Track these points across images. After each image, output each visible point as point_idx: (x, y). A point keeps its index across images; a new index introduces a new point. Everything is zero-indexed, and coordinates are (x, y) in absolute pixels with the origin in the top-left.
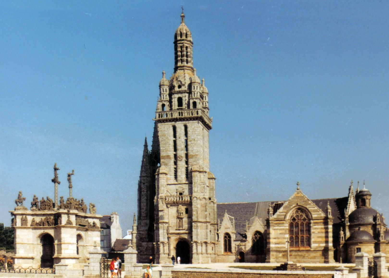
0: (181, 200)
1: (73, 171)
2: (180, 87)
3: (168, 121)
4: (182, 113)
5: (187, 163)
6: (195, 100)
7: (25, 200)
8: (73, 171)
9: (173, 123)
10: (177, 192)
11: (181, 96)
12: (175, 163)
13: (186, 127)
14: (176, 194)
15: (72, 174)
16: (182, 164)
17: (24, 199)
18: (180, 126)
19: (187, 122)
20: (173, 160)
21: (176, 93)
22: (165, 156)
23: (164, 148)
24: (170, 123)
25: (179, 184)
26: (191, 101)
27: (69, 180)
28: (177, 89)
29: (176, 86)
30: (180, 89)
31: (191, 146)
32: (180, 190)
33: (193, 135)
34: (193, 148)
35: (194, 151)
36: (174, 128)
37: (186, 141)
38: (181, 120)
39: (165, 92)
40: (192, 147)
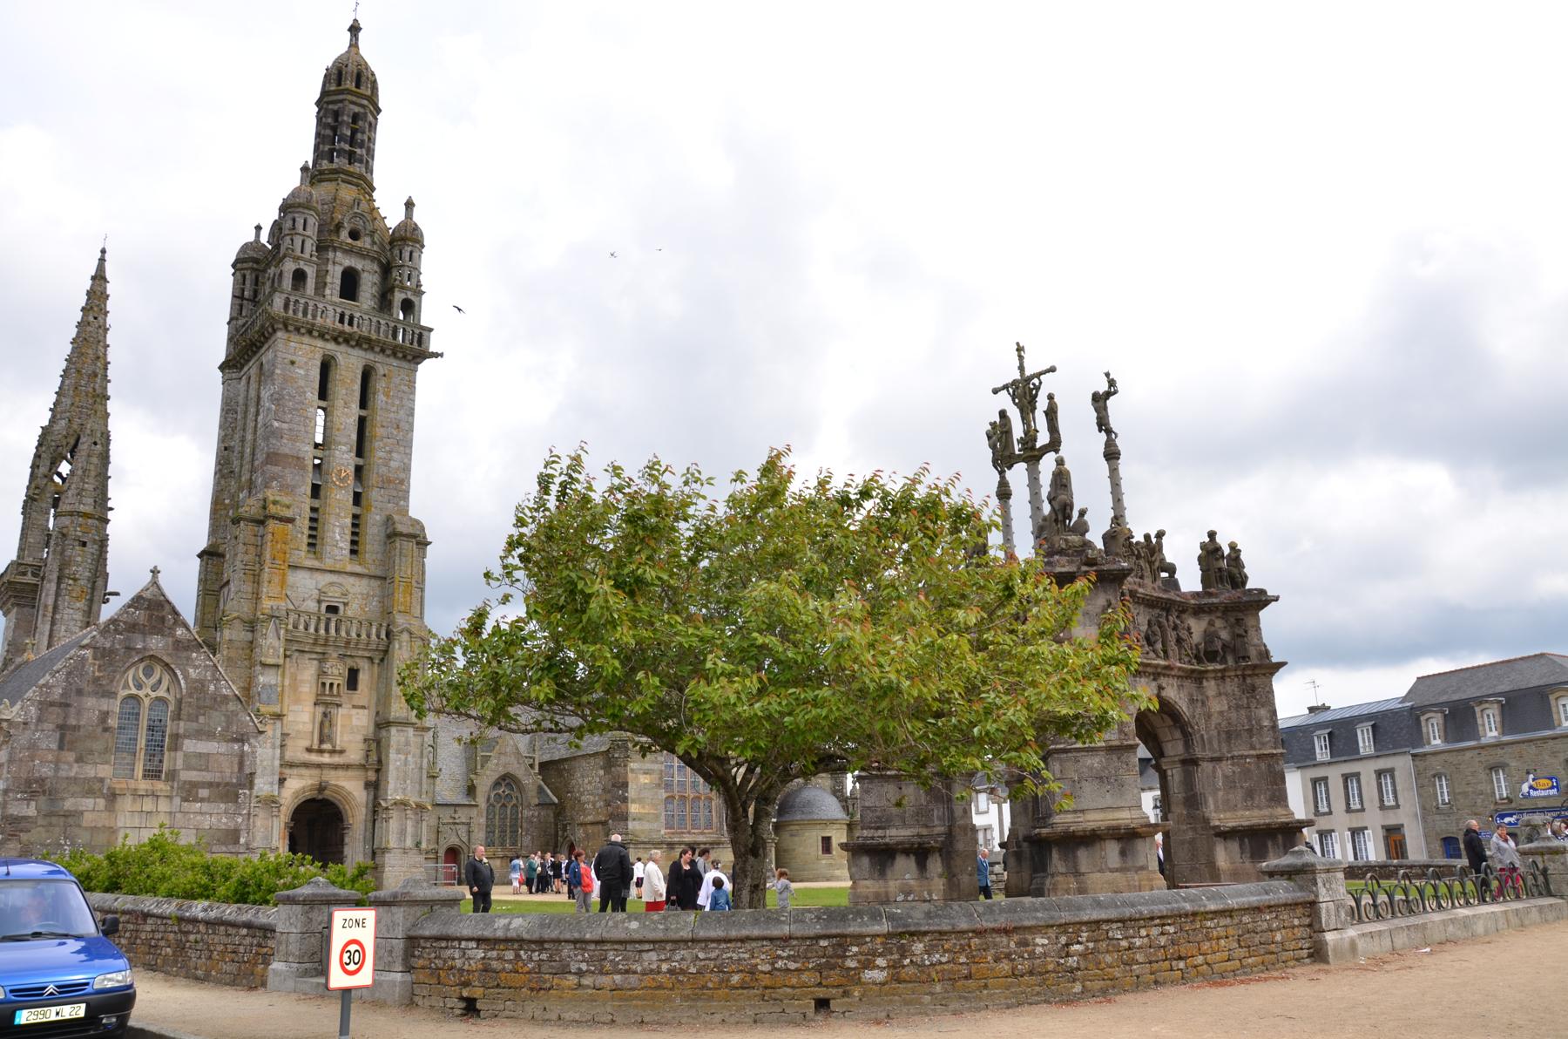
0: (322, 632)
2: (354, 235)
3: (316, 334)
4: (342, 321)
5: (357, 499)
6: (410, 295)
9: (331, 346)
10: (319, 602)
11: (359, 267)
12: (316, 491)
13: (367, 375)
14: (316, 605)
16: (340, 499)
18: (350, 363)
19: (379, 358)
20: (309, 478)
21: (346, 252)
22: (286, 456)
23: (285, 426)
24: (320, 343)
25: (331, 571)
26: (398, 297)
28: (344, 235)
29: (347, 226)
30: (358, 243)
31: (386, 445)
32: (334, 597)
33: (394, 409)
34: (390, 452)
35: (393, 464)
36: (326, 367)
37: (362, 421)
38: (362, 342)
39: (309, 232)
40: (387, 448)
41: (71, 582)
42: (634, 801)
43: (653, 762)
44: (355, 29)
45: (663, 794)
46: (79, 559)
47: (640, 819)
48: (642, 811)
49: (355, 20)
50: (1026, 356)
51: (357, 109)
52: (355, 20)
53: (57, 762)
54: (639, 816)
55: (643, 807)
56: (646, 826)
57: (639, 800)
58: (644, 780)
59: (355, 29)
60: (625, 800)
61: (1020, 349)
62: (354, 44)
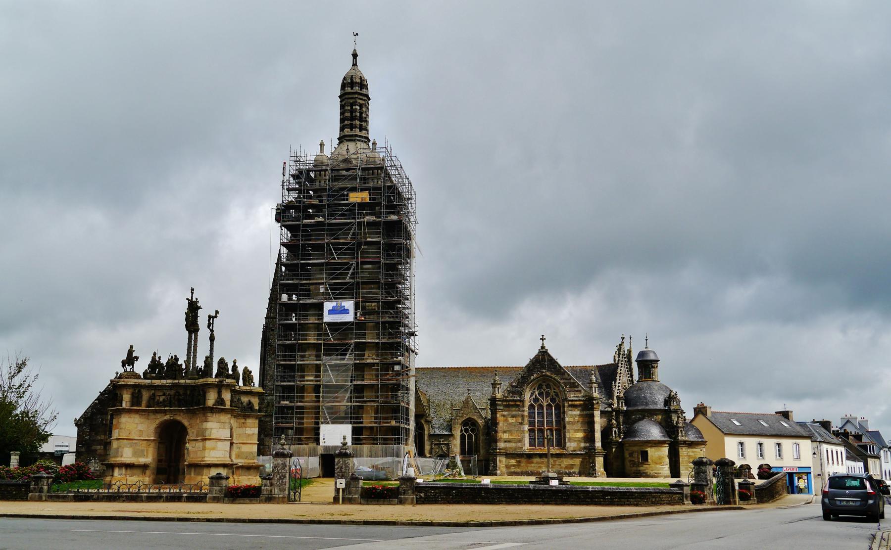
1: (217, 312)
7: (137, 361)
8: (217, 312)
15: (216, 317)
17: (137, 358)
27: (210, 325)
41: (269, 347)
42: (504, 432)
43: (517, 411)
44: (355, 56)
45: (526, 427)
46: (272, 337)
47: (509, 441)
48: (510, 437)
49: (355, 50)
50: (194, 292)
51: (351, 101)
52: (355, 50)
53: (89, 435)
54: (508, 439)
55: (511, 435)
56: (513, 445)
57: (510, 432)
58: (511, 420)
59: (355, 56)
60: (496, 432)
61: (192, 290)
62: (355, 64)
